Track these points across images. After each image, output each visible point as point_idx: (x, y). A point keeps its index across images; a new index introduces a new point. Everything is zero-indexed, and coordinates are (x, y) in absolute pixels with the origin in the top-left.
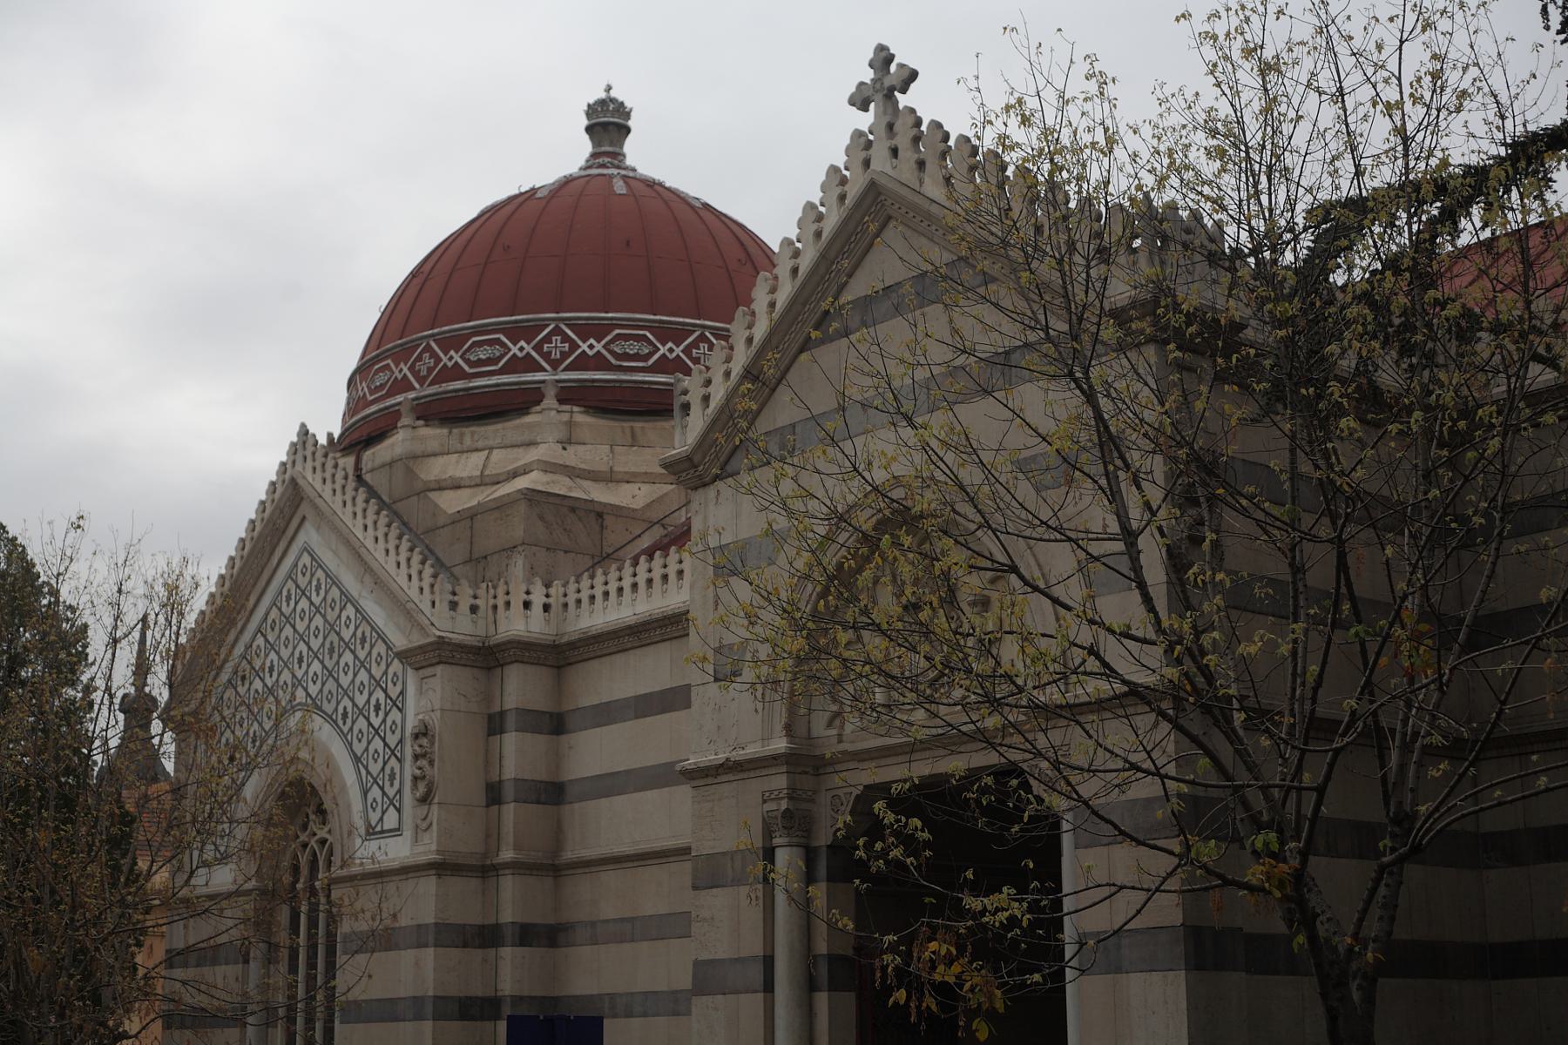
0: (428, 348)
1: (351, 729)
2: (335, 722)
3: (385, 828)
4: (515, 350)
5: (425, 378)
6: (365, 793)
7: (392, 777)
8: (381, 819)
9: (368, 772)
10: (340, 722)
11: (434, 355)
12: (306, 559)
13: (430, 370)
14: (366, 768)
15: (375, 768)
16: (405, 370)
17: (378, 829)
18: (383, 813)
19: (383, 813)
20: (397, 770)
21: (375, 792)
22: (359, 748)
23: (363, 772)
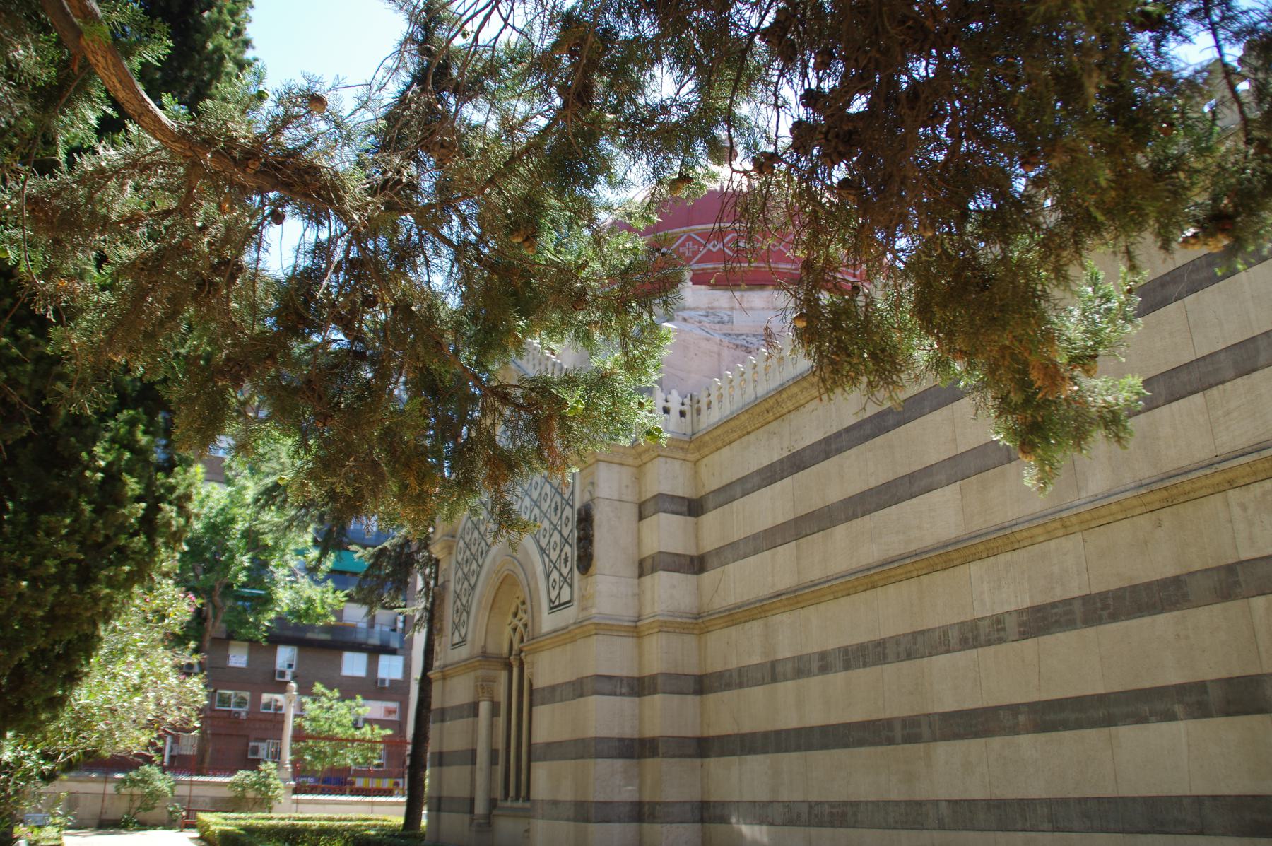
3: (562, 601)
6: (548, 576)
8: (559, 594)
9: (551, 561)
14: (548, 556)
15: (554, 555)
17: (557, 603)
18: (560, 589)
19: (560, 589)
20: (569, 555)
21: (555, 575)
22: (544, 542)
23: (547, 560)
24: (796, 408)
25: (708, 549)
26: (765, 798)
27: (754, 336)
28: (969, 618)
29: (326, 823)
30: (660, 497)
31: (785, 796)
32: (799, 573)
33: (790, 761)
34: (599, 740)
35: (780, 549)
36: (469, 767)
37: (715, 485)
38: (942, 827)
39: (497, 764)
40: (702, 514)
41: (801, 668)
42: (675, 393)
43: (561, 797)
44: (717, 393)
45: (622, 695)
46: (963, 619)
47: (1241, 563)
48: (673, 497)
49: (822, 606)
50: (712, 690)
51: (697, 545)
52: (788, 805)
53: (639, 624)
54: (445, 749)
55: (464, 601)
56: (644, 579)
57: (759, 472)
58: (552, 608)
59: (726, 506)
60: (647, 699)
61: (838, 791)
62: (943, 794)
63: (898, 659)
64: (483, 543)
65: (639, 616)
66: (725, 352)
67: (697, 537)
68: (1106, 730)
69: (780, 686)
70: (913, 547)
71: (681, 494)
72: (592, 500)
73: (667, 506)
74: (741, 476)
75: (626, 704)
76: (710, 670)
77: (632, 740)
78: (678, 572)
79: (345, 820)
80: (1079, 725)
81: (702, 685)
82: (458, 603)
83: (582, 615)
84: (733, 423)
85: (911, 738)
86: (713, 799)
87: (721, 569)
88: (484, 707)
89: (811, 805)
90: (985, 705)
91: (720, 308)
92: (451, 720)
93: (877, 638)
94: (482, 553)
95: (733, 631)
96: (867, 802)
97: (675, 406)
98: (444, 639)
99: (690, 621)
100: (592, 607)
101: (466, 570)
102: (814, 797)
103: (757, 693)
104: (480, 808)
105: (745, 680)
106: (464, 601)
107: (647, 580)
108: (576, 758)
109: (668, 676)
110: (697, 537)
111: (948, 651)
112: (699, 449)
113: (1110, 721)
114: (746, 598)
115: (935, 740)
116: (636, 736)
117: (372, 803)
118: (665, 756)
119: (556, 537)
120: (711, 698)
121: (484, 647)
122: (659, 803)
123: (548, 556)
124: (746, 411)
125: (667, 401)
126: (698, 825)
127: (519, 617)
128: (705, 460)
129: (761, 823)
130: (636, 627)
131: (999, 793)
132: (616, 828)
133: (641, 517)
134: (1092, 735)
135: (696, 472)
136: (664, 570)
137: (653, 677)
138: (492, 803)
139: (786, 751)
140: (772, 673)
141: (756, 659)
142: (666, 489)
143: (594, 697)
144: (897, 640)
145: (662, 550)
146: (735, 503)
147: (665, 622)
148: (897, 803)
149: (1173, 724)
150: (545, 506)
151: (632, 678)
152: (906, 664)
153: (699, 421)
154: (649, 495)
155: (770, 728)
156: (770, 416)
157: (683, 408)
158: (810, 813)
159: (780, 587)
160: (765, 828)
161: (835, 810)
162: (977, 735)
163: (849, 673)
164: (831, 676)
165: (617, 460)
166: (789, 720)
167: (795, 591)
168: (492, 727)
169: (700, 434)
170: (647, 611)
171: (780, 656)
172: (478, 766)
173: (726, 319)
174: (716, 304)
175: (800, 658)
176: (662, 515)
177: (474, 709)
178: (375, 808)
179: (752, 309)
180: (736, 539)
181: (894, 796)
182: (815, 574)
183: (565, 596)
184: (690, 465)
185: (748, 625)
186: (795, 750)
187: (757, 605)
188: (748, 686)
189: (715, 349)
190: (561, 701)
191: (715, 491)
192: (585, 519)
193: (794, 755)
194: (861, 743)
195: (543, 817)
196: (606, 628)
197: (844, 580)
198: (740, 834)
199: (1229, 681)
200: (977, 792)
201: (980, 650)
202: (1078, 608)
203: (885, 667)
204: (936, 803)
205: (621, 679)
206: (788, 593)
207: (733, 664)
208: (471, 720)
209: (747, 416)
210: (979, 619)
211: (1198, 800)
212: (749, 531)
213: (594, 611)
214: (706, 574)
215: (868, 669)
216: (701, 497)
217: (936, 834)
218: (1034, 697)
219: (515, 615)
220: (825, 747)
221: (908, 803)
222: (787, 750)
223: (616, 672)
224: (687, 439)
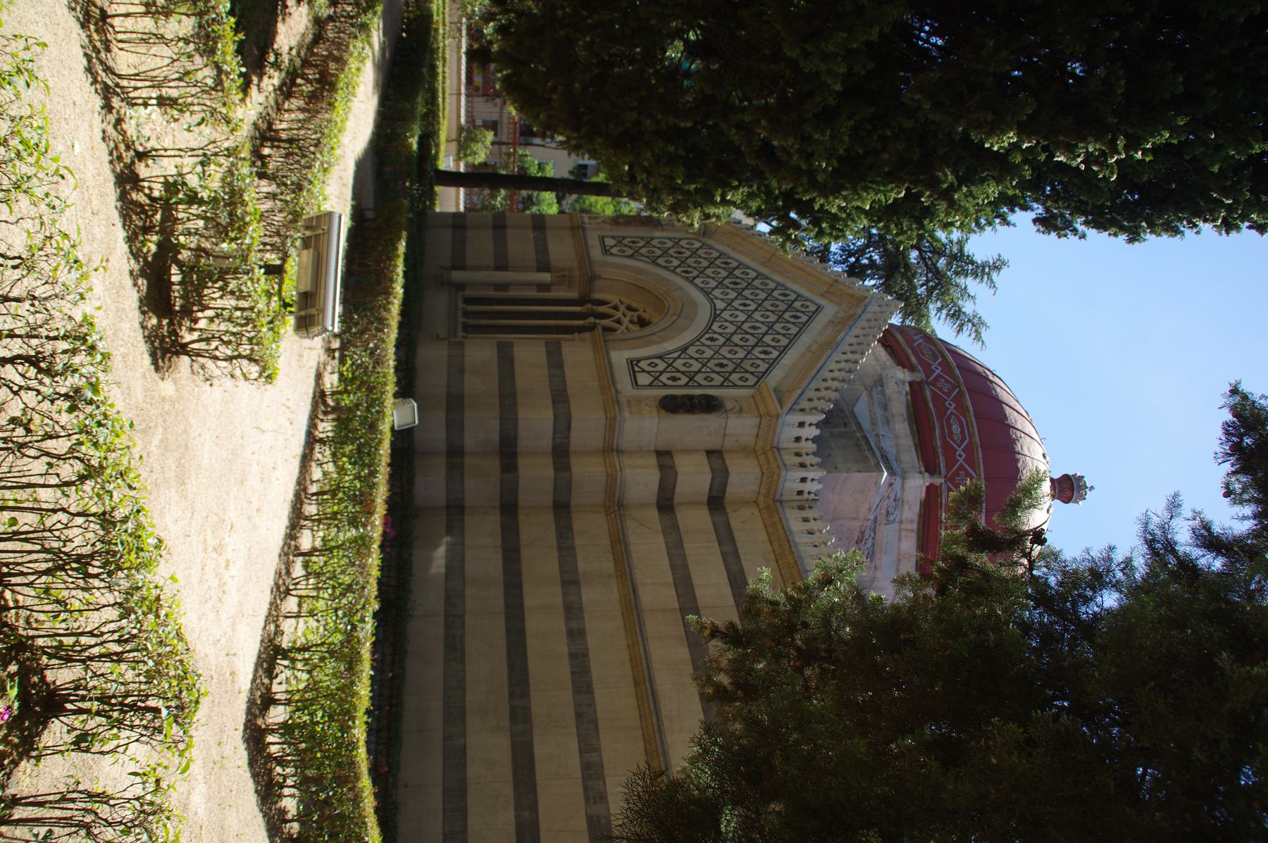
0: (954, 387)
1: (704, 345)
2: (707, 332)
3: (637, 374)
4: (960, 451)
5: (935, 386)
6: (661, 357)
7: (674, 379)
8: (644, 371)
9: (675, 359)
10: (707, 336)
11: (950, 391)
12: (813, 308)
13: (940, 389)
14: (679, 357)
15: (679, 364)
16: (938, 371)
17: (636, 369)
18: (648, 372)
19: (648, 372)
20: (679, 383)
21: (662, 366)
22: (691, 351)
23: (675, 355)
25: (679, 516)
27: (873, 544)
28: (606, 772)
29: (440, 78)
31: (470, 592)
33: (496, 598)
35: (673, 592)
36: (492, 263)
37: (735, 523)
38: (446, 738)
40: (710, 509)
41: (573, 610)
42: (820, 486)
43: (467, 376)
44: (816, 528)
45: (554, 438)
46: (606, 766)
48: (725, 484)
50: (557, 518)
51: (682, 504)
53: (615, 453)
54: (509, 232)
55: (643, 251)
56: (654, 456)
57: (742, 572)
58: (631, 362)
59: (714, 535)
60: (550, 461)
62: (471, 740)
63: (577, 705)
64: (696, 273)
65: (622, 451)
66: (857, 524)
67: (691, 503)
69: (558, 590)
70: (666, 723)
71: (728, 490)
72: (726, 411)
74: (740, 551)
75: (547, 442)
76: (574, 516)
77: (515, 446)
78: (659, 490)
79: (444, 77)
81: (562, 508)
82: (642, 243)
83: (623, 400)
84: (786, 547)
85: (513, 712)
86: (466, 517)
87: (660, 529)
88: (546, 277)
90: (538, 783)
91: (902, 511)
92: (535, 238)
93: (594, 686)
94: (687, 272)
95: (606, 541)
96: (464, 671)
97: (807, 487)
98: (608, 226)
99: (616, 499)
100: (631, 413)
101: (671, 251)
102: (469, 620)
103: (552, 567)
104: (457, 275)
106: (643, 251)
107: (652, 461)
108: (500, 395)
109: (569, 481)
110: (691, 503)
111: (581, 751)
114: (634, 555)
115: (512, 736)
116: (519, 450)
117: (459, 94)
119: (696, 366)
120: (549, 517)
121: (599, 277)
122: (462, 475)
123: (679, 357)
124: (796, 562)
125: (812, 480)
127: (628, 312)
128: (757, 513)
130: (612, 450)
132: (442, 434)
133: (709, 453)
135: (747, 503)
136: (661, 479)
137: (568, 468)
138: (461, 286)
140: (570, 581)
141: (581, 565)
142: (733, 479)
143: (552, 416)
144: (592, 704)
145: (679, 477)
146: (716, 544)
147: (616, 480)
148: (463, 699)
150: (724, 351)
151: (568, 446)
152: (571, 712)
153: (793, 508)
154: (728, 462)
157: (806, 493)
159: (642, 591)
160: (443, 570)
162: (515, 774)
164: (565, 640)
165: (761, 433)
166: (530, 600)
167: (637, 608)
168: (528, 285)
169: (780, 512)
170: (626, 461)
171: (584, 590)
172: (494, 273)
173: (891, 518)
174: (906, 507)
175: (581, 609)
176: (710, 476)
177: (544, 266)
178: (455, 97)
179: (900, 539)
180: (686, 546)
181: (469, 697)
182: (650, 627)
183: (644, 379)
185: (610, 557)
186: (505, 603)
187: (627, 569)
188: (560, 556)
189: (861, 515)
190: (550, 376)
191: (729, 523)
192: (709, 405)
193: (502, 602)
194: (511, 667)
195: (450, 356)
196: (612, 425)
198: (436, 546)
200: (473, 771)
201: (580, 780)
203: (571, 692)
204: (464, 735)
205: (568, 437)
207: (579, 542)
208: (534, 264)
209: (792, 561)
210: (604, 781)
212: (691, 559)
213: (627, 415)
214: (656, 513)
215: (569, 676)
216: (724, 508)
218: (543, 825)
219: (629, 308)
220: (508, 632)
221: (464, 708)
222: (506, 595)
223: (573, 434)
224: (777, 497)
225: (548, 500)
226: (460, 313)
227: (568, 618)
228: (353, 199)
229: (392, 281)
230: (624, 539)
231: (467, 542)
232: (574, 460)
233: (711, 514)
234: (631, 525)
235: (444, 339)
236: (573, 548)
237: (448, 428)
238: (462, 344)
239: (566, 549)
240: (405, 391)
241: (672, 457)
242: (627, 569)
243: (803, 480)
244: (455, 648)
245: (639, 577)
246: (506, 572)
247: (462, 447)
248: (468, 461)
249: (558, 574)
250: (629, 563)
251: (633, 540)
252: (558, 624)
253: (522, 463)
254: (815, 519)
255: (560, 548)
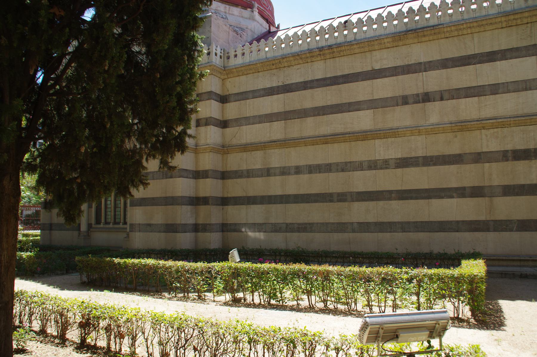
24: (289, 66)
26: (261, 221)
27: (237, 27)
28: (373, 159)
30: (211, 92)
31: (273, 221)
32: (285, 134)
34: (182, 197)
35: (275, 123)
37: (236, 91)
38: (354, 231)
39: (92, 207)
40: (226, 103)
41: (284, 171)
42: (218, 46)
43: (153, 222)
44: (242, 51)
45: (190, 178)
46: (370, 159)
47: (483, 152)
48: (216, 93)
49: (298, 148)
50: (229, 178)
51: (223, 116)
52: (274, 225)
53: (198, 147)
56: (199, 128)
57: (264, 89)
60: (201, 180)
61: (303, 219)
62: (355, 220)
63: (337, 171)
65: (196, 144)
68: (427, 200)
70: (348, 130)
71: (218, 93)
73: (214, 97)
74: (252, 89)
80: (417, 198)
81: (224, 175)
84: (252, 66)
86: (229, 222)
89: (287, 224)
90: (378, 190)
91: (221, 11)
95: (245, 154)
96: (317, 223)
99: (221, 148)
102: (289, 221)
103: (259, 181)
105: (251, 175)
111: (362, 170)
112: (227, 74)
113: (429, 198)
114: (253, 141)
116: (194, 196)
118: (213, 205)
120: (230, 182)
122: (210, 224)
124: (262, 63)
125: (216, 50)
126: (221, 233)
128: (230, 80)
129: (259, 231)
130: (196, 149)
131: (381, 220)
132: (188, 235)
134: (421, 202)
138: (90, 226)
139: (274, 203)
140: (268, 172)
141: (258, 166)
144: (337, 164)
146: (248, 101)
147: (214, 148)
149: (452, 199)
152: (341, 174)
154: (204, 91)
155: (264, 194)
156: (274, 67)
158: (286, 227)
159: (274, 138)
160: (262, 234)
161: (301, 226)
163: (311, 175)
164: (301, 176)
167: (285, 141)
173: (224, 16)
174: (219, 9)
175: (284, 168)
176: (212, 100)
179: (233, 15)
181: (332, 221)
182: (295, 135)
184: (221, 80)
186: (279, 203)
187: (262, 144)
188: (253, 177)
191: (235, 94)
193: (279, 205)
194: (316, 201)
197: (313, 139)
198: (247, 236)
199: (473, 187)
201: (377, 171)
202: (421, 160)
203: (330, 174)
206: (279, 141)
207: (244, 167)
209: (261, 64)
210: (377, 160)
211: (458, 222)
212: (256, 114)
214: (228, 129)
215: (321, 174)
216: (226, 95)
217: (351, 234)
218: (399, 188)
223: (188, 168)
225: (220, 181)
226: (107, 226)
227: (289, 174)
228: (90, 290)
229: (145, 266)
230: (245, 145)
231: (244, 221)
232: (201, 168)
233: (229, 102)
234: (235, 142)
235: (128, 235)
236: (248, 171)
237: (186, 232)
238: (132, 225)
239: (249, 174)
240: (223, 256)
241: (201, 119)
242: (262, 144)
243: (216, 54)
244: (304, 228)
245: (266, 139)
246: (261, 203)
247: (193, 224)
248: (200, 221)
249: (263, 178)
250: (258, 144)
251: (244, 141)
252: (292, 178)
253: (202, 194)
254: (236, 51)
255: (248, 177)
